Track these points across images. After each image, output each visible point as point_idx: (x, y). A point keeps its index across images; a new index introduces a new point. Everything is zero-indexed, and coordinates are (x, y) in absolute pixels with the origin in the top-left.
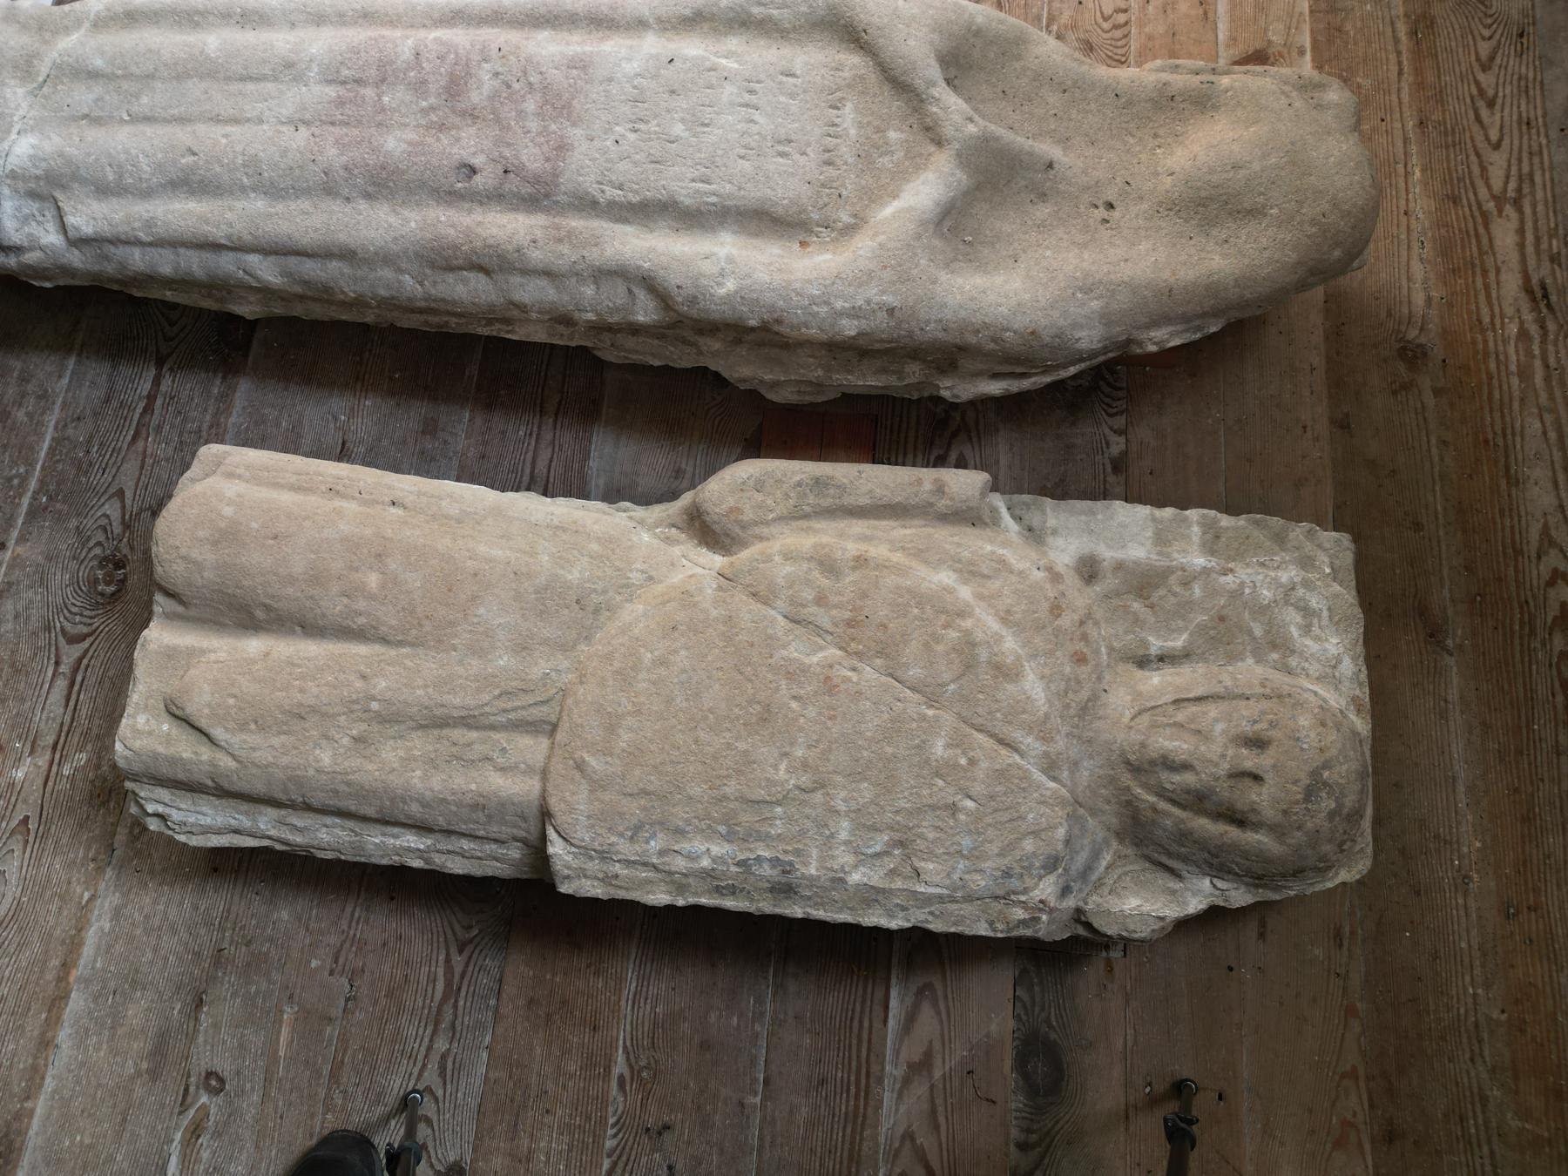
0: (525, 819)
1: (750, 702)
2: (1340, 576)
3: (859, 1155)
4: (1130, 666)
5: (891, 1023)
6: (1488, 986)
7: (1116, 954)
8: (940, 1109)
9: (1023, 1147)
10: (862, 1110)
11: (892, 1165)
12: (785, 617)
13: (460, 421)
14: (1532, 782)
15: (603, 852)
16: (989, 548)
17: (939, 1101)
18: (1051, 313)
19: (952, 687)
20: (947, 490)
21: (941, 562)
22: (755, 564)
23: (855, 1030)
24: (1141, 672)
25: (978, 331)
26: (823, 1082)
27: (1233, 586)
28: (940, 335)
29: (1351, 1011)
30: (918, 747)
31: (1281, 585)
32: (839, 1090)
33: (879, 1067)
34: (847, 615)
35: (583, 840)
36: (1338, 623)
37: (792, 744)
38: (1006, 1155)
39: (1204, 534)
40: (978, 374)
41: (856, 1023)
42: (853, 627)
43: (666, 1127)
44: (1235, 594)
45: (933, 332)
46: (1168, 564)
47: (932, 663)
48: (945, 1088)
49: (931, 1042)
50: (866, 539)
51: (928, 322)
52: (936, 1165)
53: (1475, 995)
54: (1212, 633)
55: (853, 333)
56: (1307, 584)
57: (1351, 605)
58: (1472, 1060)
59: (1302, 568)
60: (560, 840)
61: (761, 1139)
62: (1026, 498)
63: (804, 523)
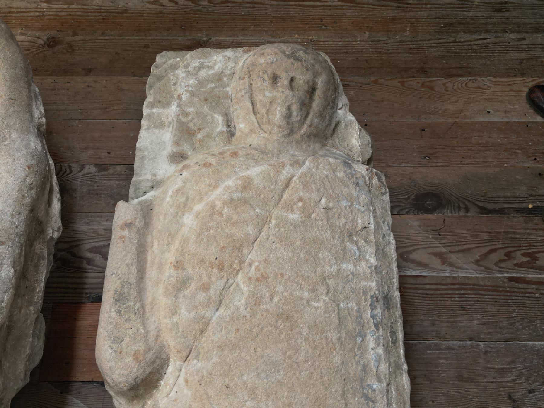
1: (277, 328)
3: (494, 286)
4: (234, 139)
5: (424, 274)
6: (356, 37)
8: (460, 248)
9: (467, 210)
10: (471, 286)
11: (493, 270)
12: (217, 309)
14: (268, 16)
17: (457, 248)
18: (16, 157)
20: (129, 222)
21: (177, 222)
22: (179, 334)
23: (432, 292)
25: (23, 196)
26: (463, 308)
27: (188, 95)
28: (22, 217)
29: (376, 82)
30: (295, 227)
31: (187, 76)
32: (465, 299)
33: (448, 278)
34: (215, 271)
37: (301, 299)
38: (473, 217)
39: (157, 107)
40: (47, 213)
41: (429, 292)
42: (223, 267)
43: (510, 397)
44: (192, 94)
45: (20, 221)
46: (175, 122)
47: (244, 221)
48: (450, 246)
49: (429, 254)
50: (161, 267)
51: (12, 223)
52: (487, 249)
53: (360, 41)
54: (213, 104)
55: (12, 270)
56: (186, 67)
58: (387, 44)
61: (500, 340)
62: (131, 190)
63: (148, 308)
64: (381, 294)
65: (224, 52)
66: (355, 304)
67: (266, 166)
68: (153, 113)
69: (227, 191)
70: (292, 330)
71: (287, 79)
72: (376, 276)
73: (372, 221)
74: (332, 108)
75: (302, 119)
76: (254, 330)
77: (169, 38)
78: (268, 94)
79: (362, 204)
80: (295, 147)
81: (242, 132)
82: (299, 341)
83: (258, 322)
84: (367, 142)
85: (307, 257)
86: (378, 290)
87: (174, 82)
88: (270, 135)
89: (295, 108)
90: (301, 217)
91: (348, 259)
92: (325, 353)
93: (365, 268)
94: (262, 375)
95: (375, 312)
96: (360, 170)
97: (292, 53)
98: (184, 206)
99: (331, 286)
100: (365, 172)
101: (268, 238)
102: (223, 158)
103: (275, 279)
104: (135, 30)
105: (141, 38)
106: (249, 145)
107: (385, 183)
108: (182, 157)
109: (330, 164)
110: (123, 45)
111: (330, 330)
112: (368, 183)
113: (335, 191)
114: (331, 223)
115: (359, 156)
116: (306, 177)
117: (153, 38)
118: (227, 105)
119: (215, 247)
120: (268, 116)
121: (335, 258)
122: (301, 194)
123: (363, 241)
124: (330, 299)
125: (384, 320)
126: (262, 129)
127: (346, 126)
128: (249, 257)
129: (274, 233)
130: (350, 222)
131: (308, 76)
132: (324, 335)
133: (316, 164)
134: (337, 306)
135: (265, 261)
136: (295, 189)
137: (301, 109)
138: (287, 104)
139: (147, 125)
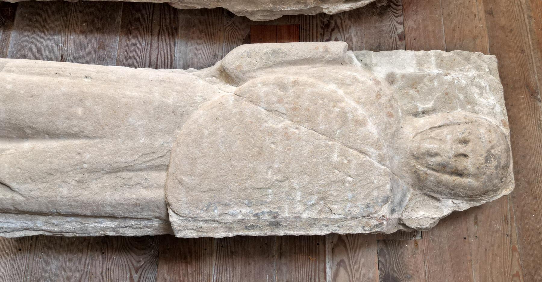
0: (158, 208)
2: (493, 72)
4: (412, 117)
7: (418, 238)
13: (115, 42)
15: (195, 218)
16: (349, 73)
19: (338, 131)
24: (416, 118)
27: (450, 80)
30: (327, 158)
31: (469, 78)
35: (185, 214)
36: (493, 90)
37: (273, 163)
39: (437, 60)
44: (451, 83)
46: (423, 73)
47: (329, 122)
54: (443, 100)
56: (480, 76)
57: (498, 83)
59: (477, 70)
60: (175, 215)
64: (280, 220)
65: (501, 105)
66: (271, 200)
67: (377, 137)
68: (430, 58)
69: (353, 109)
70: (251, 156)
71: (466, 152)
72: (293, 217)
73: (337, 217)
74: (451, 194)
76: (252, 133)
77: (535, 68)
78: (449, 137)
79: (351, 209)
80: (403, 161)
81: (416, 122)
82: (245, 162)
83: (257, 135)
84: (422, 223)
85: (303, 166)
86: (283, 218)
87: (463, 69)
88: (411, 140)
89: (438, 159)
90: (334, 162)
91: (304, 196)
92: (237, 178)
93: (298, 209)
94: (223, 139)
95: (266, 215)
96: (382, 210)
97: (493, 155)
98: (342, 83)
99: (284, 183)
100: (382, 214)
101: (317, 139)
102: (386, 107)
103: (287, 145)
104: (538, 40)
105: (531, 46)
106: (402, 126)
107: (374, 231)
108: (392, 82)
109: (385, 185)
110: (521, 34)
111: (251, 182)
112: (371, 216)
113: (359, 188)
114: (332, 184)
115: (407, 216)
116: (370, 166)
117: (533, 55)
118: (444, 110)
119: (308, 105)
120: (429, 138)
121: (304, 187)
122: (354, 162)
123: (320, 209)
124: (274, 182)
125: (261, 221)
126: (416, 135)
127: (437, 207)
128: (303, 127)
129: (321, 143)
130: (334, 199)
131: (472, 170)
132: (249, 178)
134: (269, 187)
135: (300, 138)
136: (358, 157)
137: (439, 165)
138: (440, 152)
139: (419, 55)
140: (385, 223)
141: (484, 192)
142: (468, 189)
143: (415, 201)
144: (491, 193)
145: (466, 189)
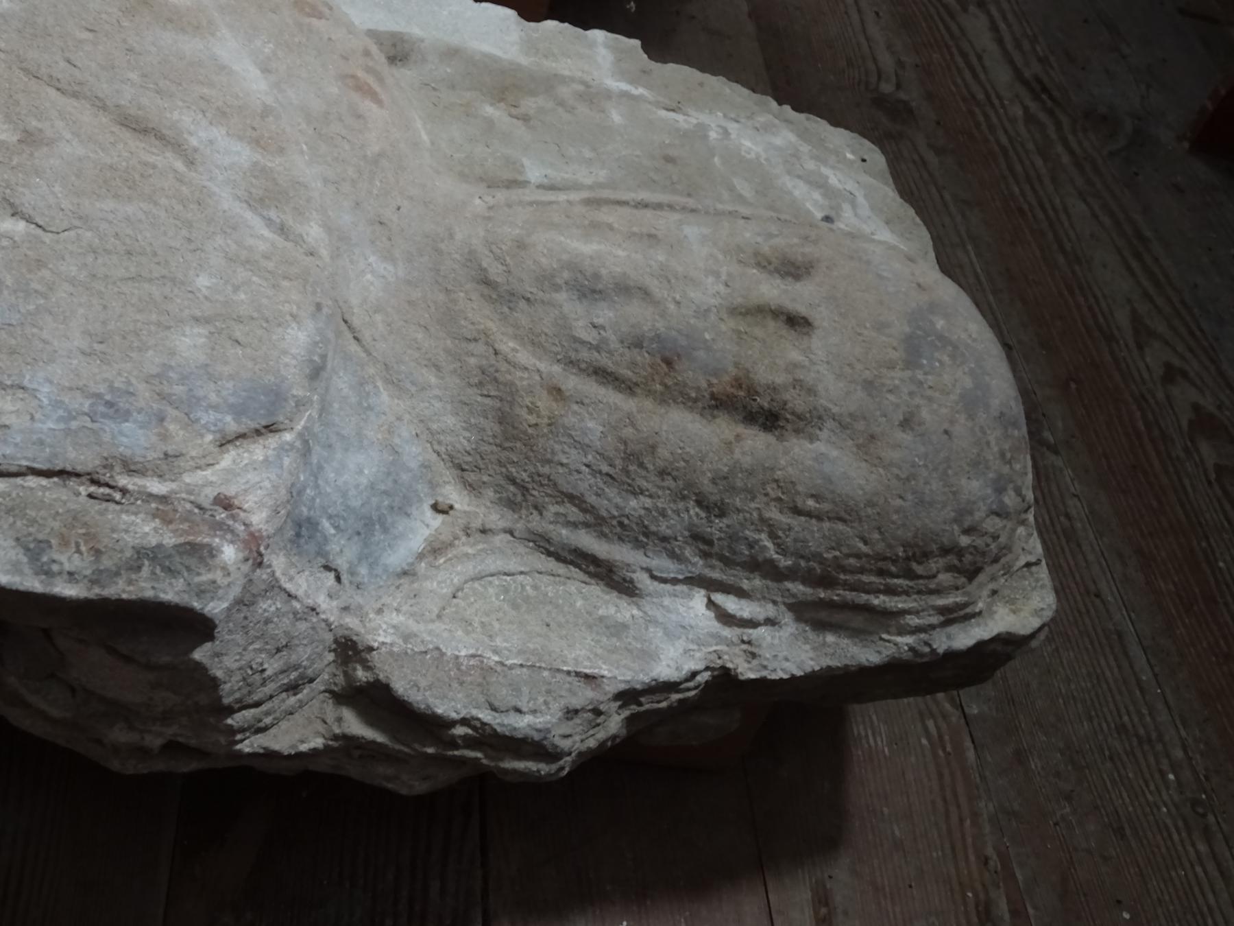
75: (585, 354)
84: (503, 696)
89: (638, 314)
107: (120, 589)
112: (123, 481)
115: (407, 638)
133: (270, 265)
137: (638, 343)
140: (229, 553)
141: (905, 545)
142: (811, 503)
143: (469, 568)
144: (945, 578)
145: (800, 504)
